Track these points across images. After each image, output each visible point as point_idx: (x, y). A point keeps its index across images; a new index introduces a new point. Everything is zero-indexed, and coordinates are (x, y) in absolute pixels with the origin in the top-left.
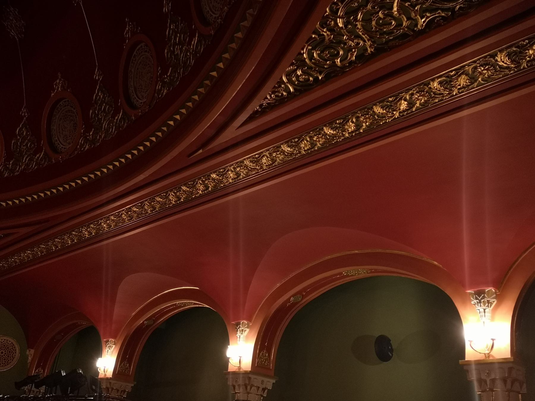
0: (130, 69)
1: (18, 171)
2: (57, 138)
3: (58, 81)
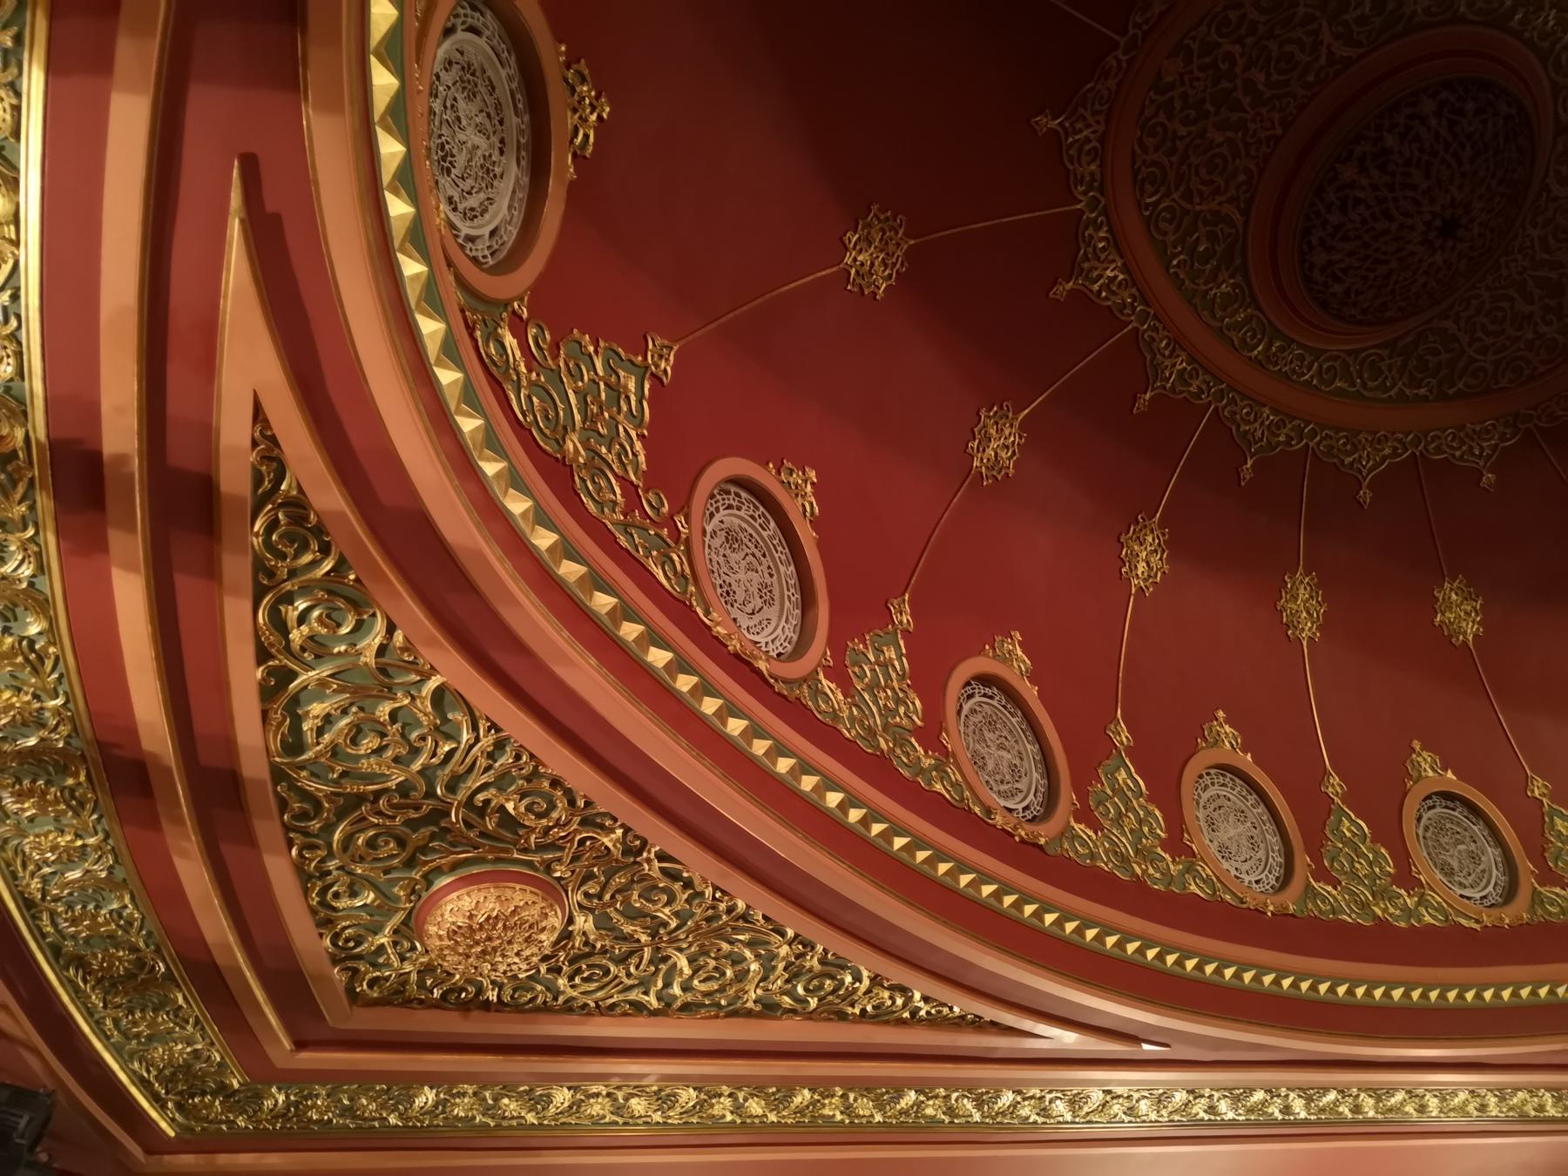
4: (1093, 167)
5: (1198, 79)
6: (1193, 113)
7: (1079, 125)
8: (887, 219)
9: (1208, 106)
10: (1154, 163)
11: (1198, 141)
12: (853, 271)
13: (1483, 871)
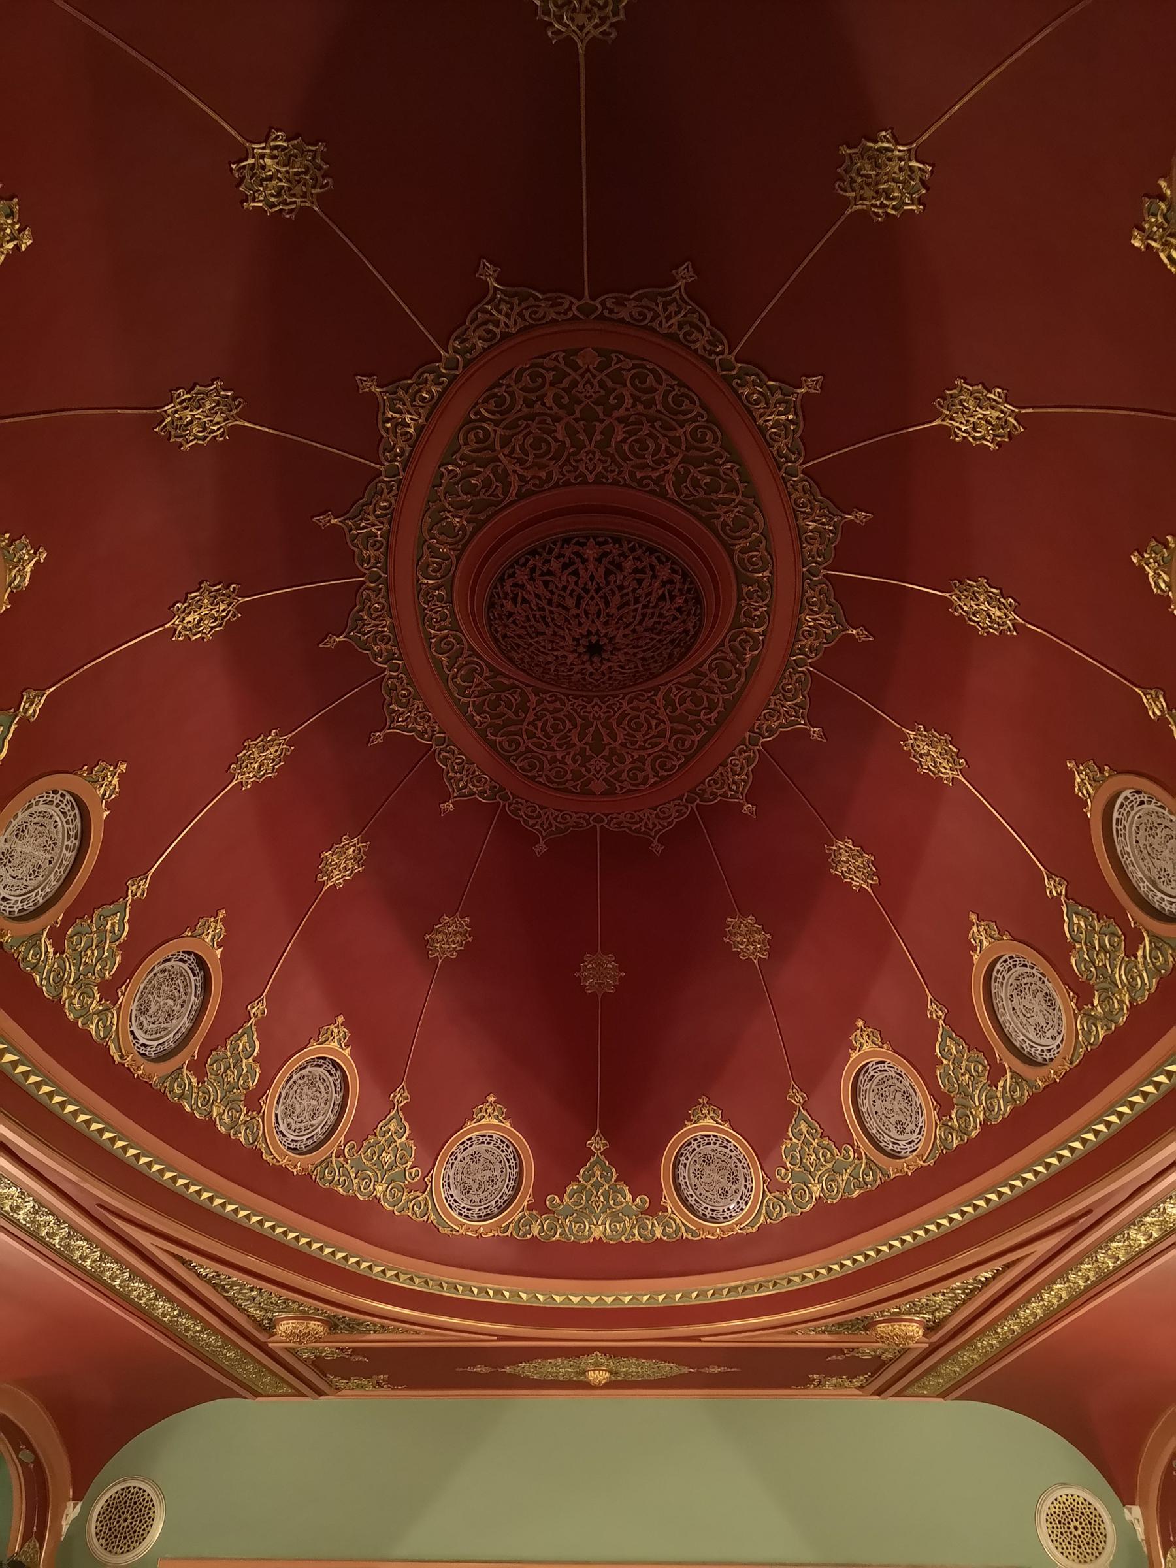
0: (1119, 850)
1: (976, 1128)
2: (1022, 1037)
3: (975, 928)
4: (480, 343)
5: (592, 386)
6: (566, 401)
7: (504, 307)
8: (320, 168)
9: (578, 409)
10: (512, 394)
11: (549, 420)
12: (251, 161)
13: (165, 1029)
